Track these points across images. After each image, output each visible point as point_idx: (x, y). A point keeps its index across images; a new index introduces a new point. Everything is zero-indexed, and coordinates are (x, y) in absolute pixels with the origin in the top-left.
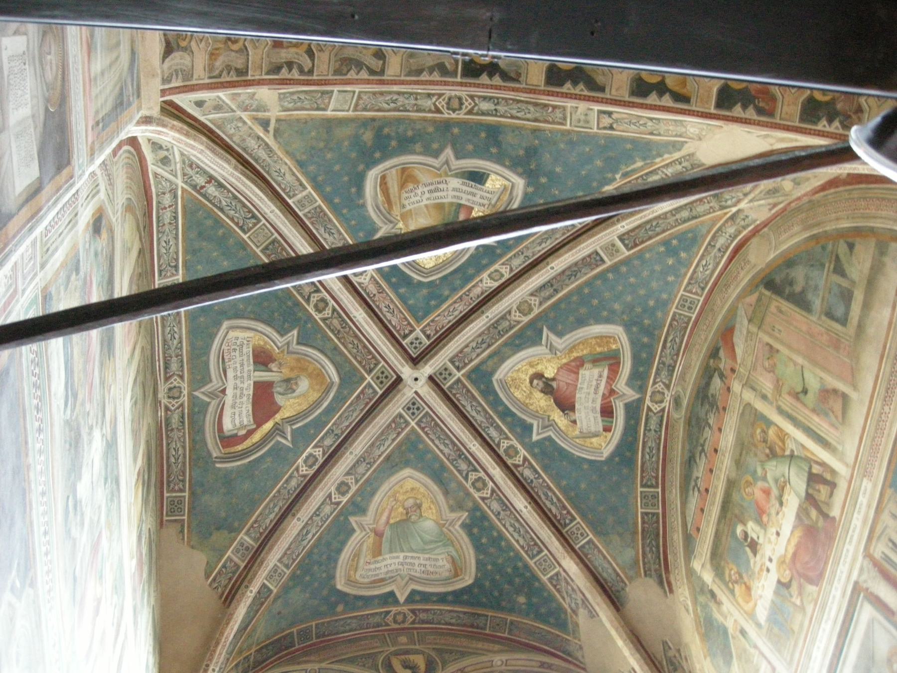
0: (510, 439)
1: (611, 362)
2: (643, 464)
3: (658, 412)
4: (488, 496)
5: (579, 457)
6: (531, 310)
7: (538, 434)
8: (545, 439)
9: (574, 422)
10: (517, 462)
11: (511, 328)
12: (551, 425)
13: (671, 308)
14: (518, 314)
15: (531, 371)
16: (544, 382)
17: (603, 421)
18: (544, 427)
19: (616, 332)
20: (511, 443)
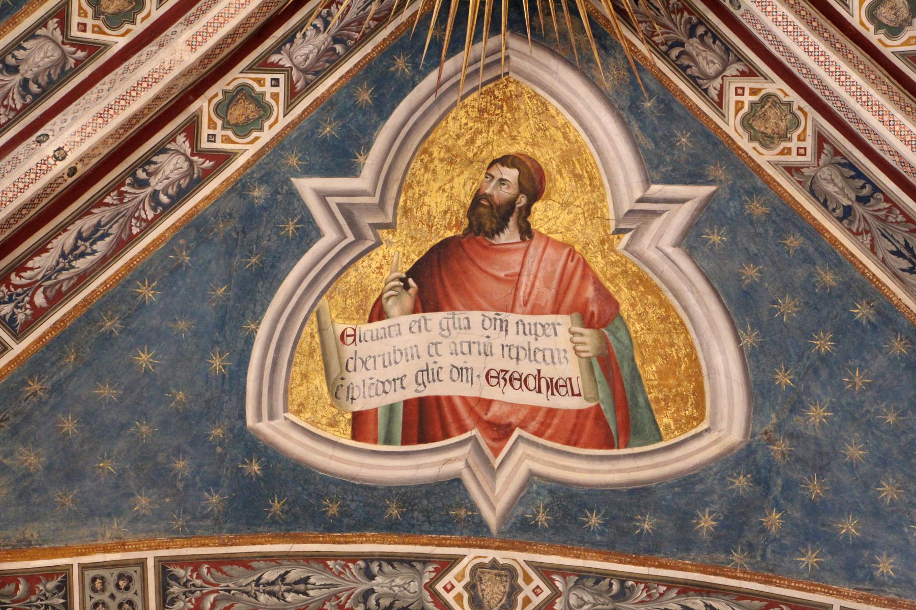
0: (288, 107)
1: (609, 416)
2: (244, 562)
3: (435, 595)
4: (75, 32)
5: (249, 341)
6: (766, 140)
7: (322, 196)
8: (307, 219)
9: (378, 313)
10: (205, 131)
11: (694, 81)
12: (359, 237)
13: (840, 594)
14: (747, 99)
15: (547, 157)
16: (511, 204)
17: (391, 408)
18: (348, 212)
19: (723, 425)
20: (278, 108)
